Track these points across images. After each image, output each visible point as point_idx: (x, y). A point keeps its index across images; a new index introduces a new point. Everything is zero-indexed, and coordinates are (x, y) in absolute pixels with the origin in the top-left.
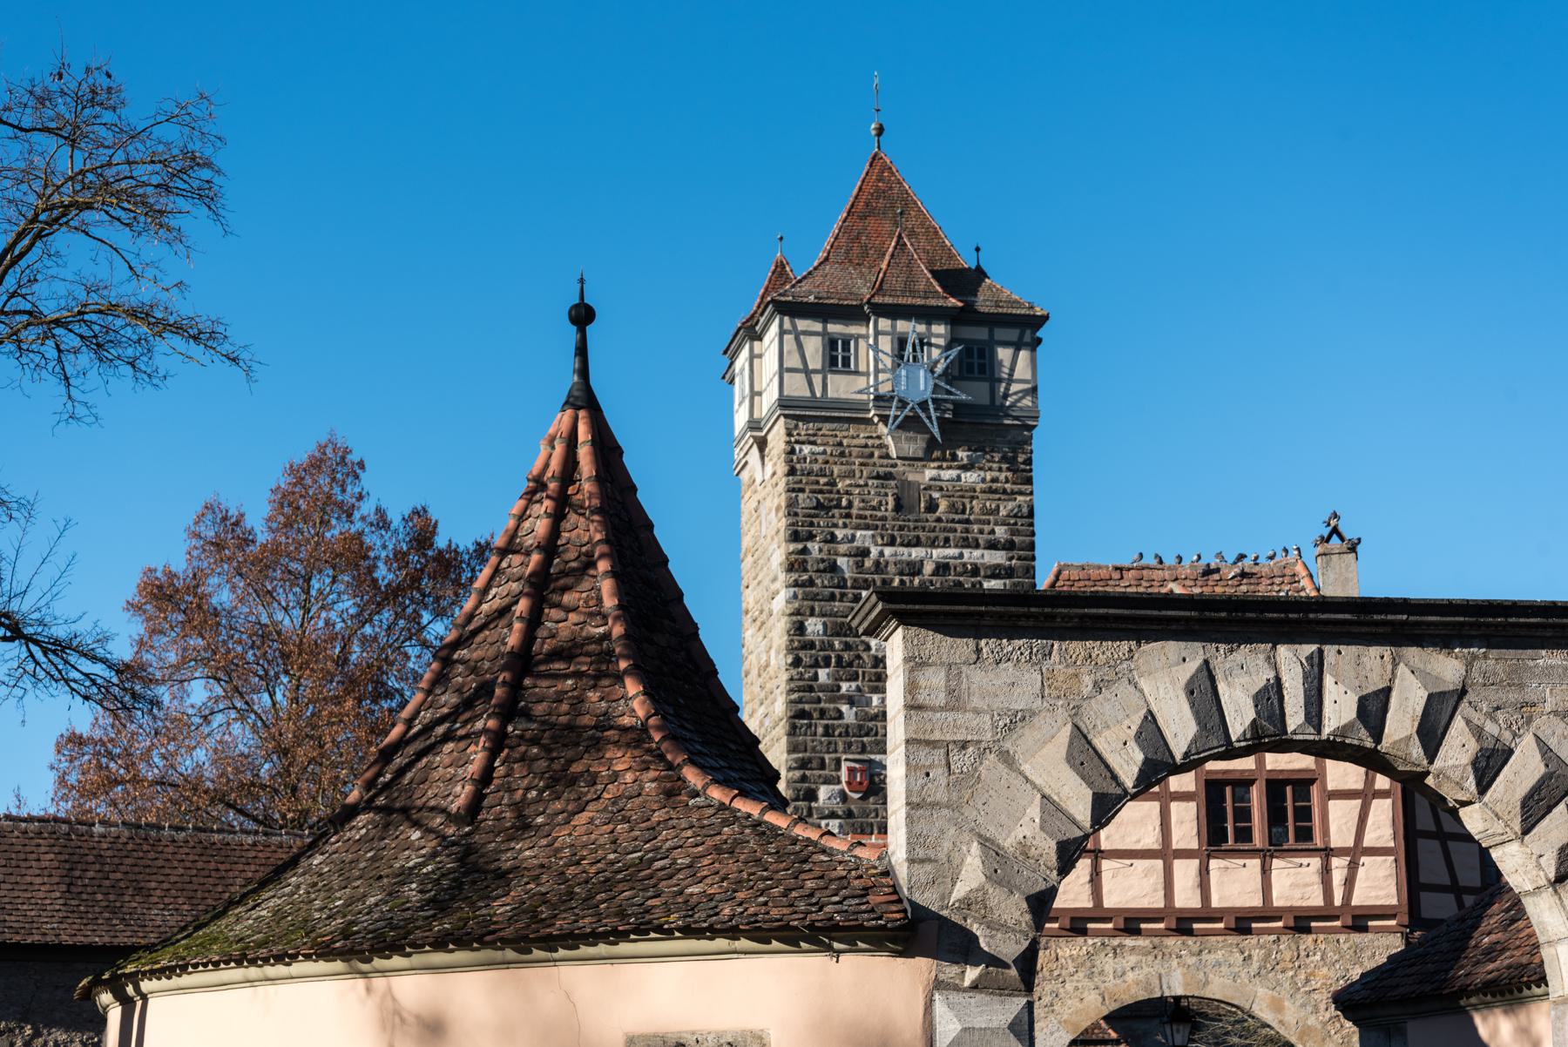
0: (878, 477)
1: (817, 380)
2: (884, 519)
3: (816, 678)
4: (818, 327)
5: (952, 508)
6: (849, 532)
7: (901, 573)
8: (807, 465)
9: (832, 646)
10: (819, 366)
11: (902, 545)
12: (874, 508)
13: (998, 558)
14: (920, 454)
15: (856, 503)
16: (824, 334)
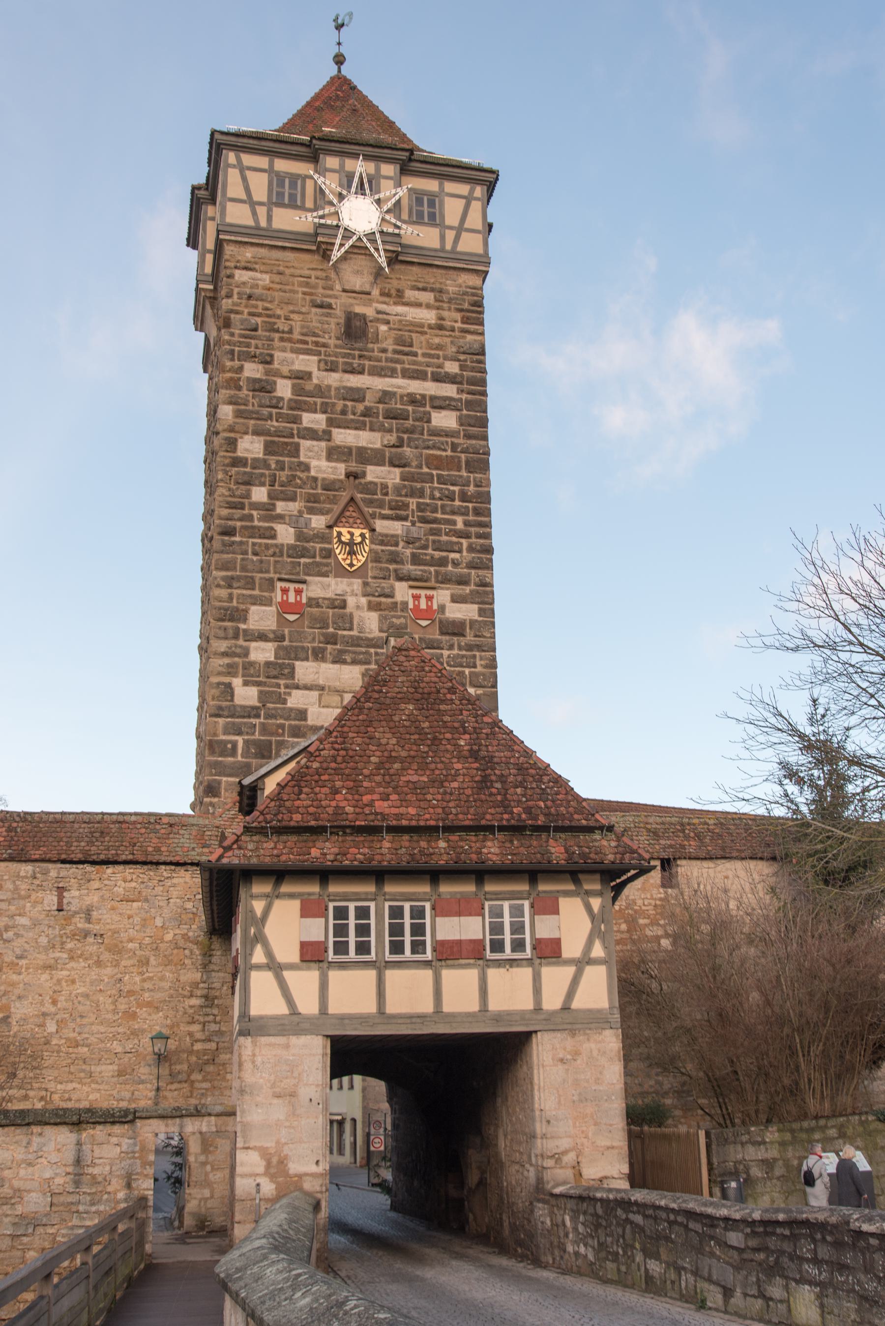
0: (321, 306)
1: (262, 211)
2: (324, 345)
3: (248, 496)
4: (262, 162)
5: (400, 341)
6: (290, 356)
7: (344, 399)
8: (248, 291)
9: (268, 467)
10: (264, 199)
11: (345, 371)
12: (315, 335)
13: (449, 390)
14: (367, 288)
15: (297, 330)
16: (270, 171)
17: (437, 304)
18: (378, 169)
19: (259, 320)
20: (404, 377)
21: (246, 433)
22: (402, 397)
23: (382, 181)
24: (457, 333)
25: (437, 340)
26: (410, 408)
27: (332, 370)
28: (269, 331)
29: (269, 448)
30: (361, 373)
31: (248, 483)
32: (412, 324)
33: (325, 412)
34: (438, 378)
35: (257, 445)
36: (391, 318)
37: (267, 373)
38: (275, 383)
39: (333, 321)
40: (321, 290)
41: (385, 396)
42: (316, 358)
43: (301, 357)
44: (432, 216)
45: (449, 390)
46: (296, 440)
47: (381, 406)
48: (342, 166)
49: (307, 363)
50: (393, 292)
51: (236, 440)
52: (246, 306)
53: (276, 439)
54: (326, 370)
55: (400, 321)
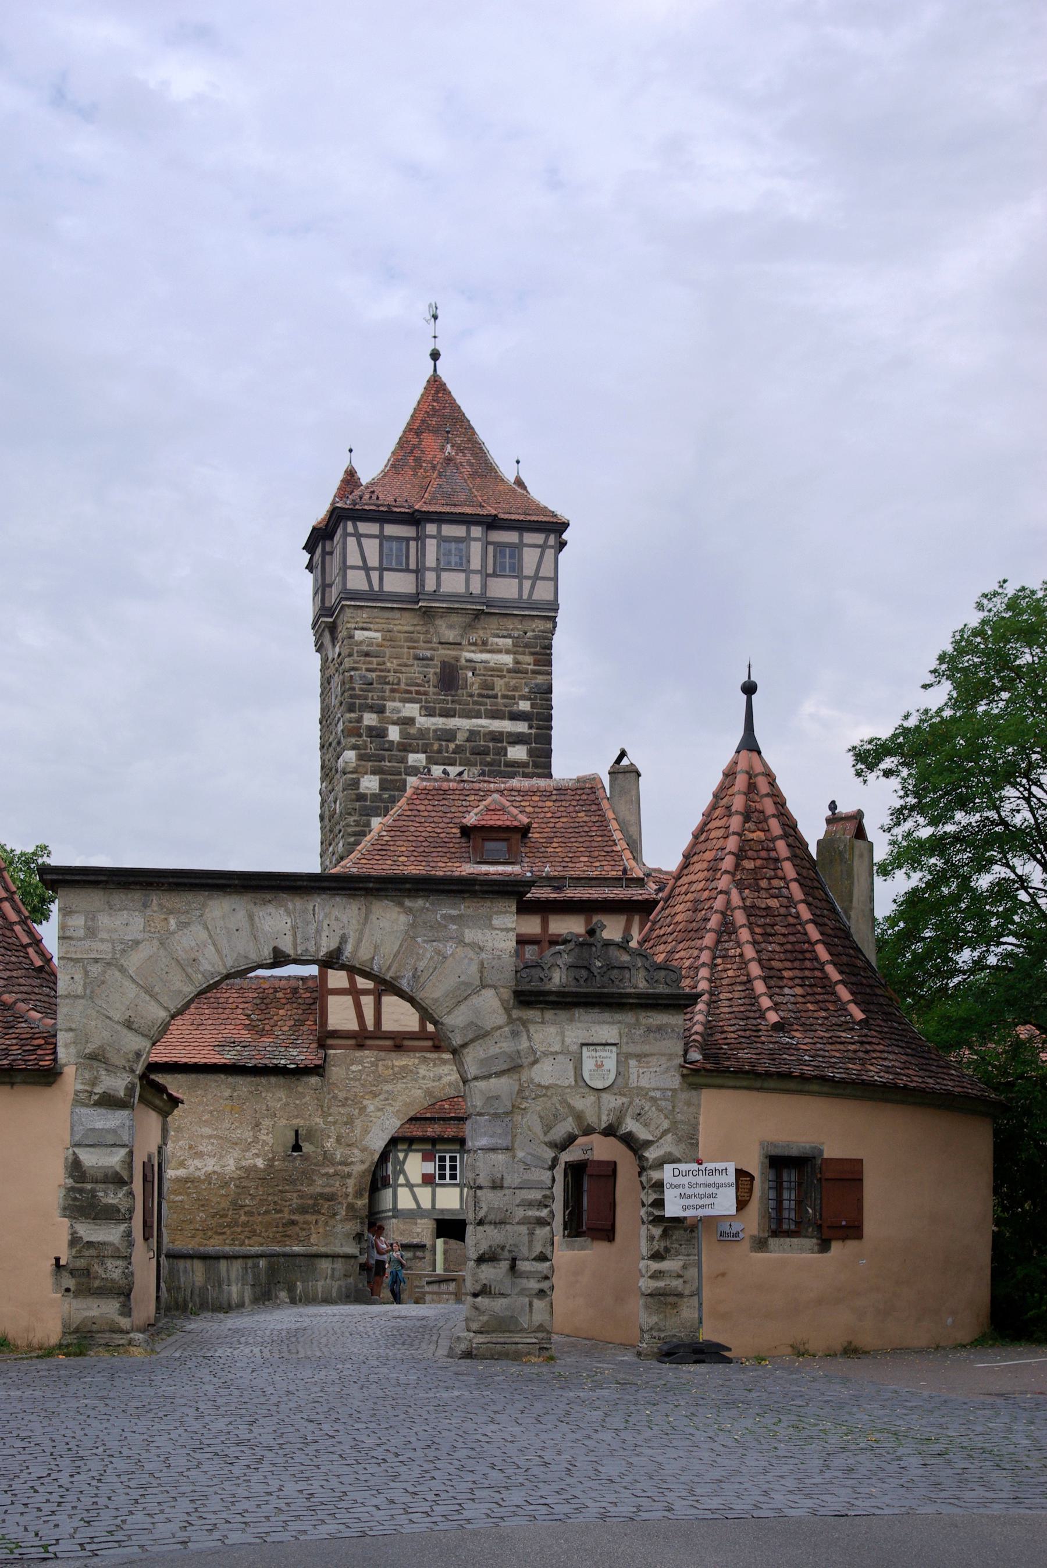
1: (375, 575)
2: (425, 693)
7: (440, 740)
8: (365, 648)
10: (377, 564)
11: (441, 716)
13: (522, 727)
16: (382, 537)
17: (515, 649)
18: (468, 531)
19: (374, 675)
20: (487, 717)
21: (366, 773)
22: (485, 735)
23: (472, 543)
24: (530, 675)
25: (513, 682)
26: (491, 745)
27: (430, 715)
28: (380, 684)
29: (382, 782)
30: (454, 716)
31: (368, 815)
32: (493, 669)
33: (425, 752)
34: (515, 717)
35: (372, 783)
36: (478, 665)
37: (380, 721)
38: (387, 729)
39: (432, 670)
40: (422, 644)
41: (473, 734)
42: (418, 706)
43: (407, 705)
44: (512, 568)
45: (522, 727)
46: (404, 776)
47: (468, 744)
48: (439, 531)
49: (411, 710)
50: (479, 642)
51: (359, 780)
52: (364, 663)
53: (389, 777)
54: (426, 715)
55: (485, 668)
